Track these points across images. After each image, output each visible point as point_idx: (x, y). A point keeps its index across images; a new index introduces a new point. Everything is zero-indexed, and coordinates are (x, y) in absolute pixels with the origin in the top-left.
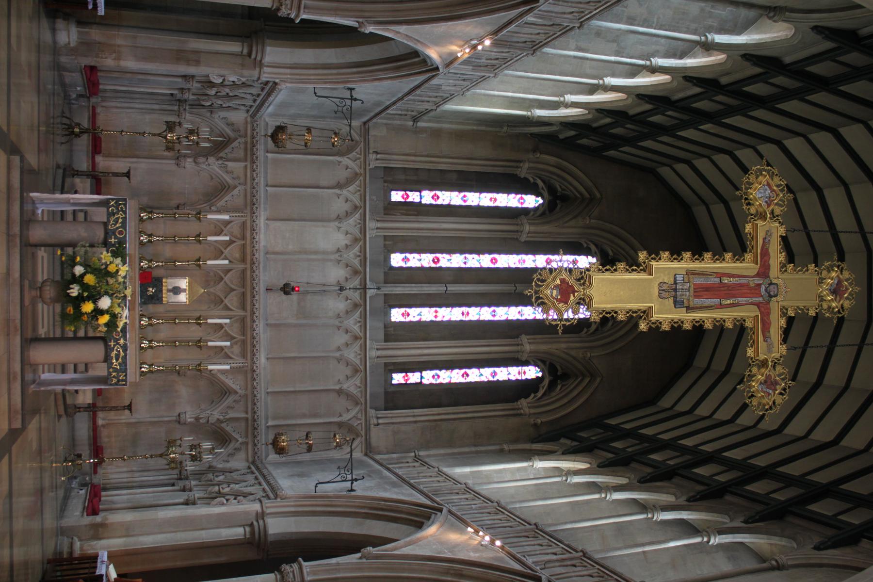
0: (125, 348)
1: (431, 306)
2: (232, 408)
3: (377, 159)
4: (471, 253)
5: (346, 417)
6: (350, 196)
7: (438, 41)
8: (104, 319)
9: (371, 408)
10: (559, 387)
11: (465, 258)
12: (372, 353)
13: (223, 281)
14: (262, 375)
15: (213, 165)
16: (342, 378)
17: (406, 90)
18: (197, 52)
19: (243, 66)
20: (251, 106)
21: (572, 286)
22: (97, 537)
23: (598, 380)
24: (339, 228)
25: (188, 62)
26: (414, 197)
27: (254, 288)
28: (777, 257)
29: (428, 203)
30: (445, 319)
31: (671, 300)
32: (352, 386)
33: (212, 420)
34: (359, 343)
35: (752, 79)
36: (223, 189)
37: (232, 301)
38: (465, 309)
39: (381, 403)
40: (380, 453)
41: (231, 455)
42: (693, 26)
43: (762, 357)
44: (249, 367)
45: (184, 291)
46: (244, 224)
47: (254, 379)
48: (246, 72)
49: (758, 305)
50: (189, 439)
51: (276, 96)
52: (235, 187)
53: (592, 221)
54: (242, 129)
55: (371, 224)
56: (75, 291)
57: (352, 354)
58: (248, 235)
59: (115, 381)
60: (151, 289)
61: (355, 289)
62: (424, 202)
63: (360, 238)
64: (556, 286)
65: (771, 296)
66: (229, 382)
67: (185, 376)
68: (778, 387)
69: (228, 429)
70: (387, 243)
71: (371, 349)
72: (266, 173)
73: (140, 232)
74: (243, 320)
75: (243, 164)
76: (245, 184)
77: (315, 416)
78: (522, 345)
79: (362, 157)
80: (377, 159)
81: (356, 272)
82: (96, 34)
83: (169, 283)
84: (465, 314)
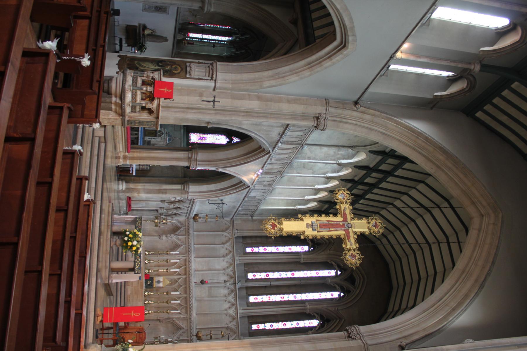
0: (140, 262)
1: (267, 295)
2: (182, 335)
3: (238, 233)
4: (282, 271)
6: (228, 247)
7: (246, 173)
8: (134, 248)
9: (241, 336)
10: (326, 325)
11: (280, 274)
12: (240, 311)
13: (177, 283)
14: (194, 320)
15: (173, 238)
16: (228, 322)
17: (242, 199)
18: (166, 190)
19: (182, 193)
20: (187, 213)
21: (276, 225)
23: (343, 320)
24: (224, 260)
25: (163, 193)
26: (256, 250)
27: (190, 285)
28: (349, 216)
29: (262, 252)
30: (274, 300)
31: (311, 229)
32: (232, 325)
34: (234, 307)
35: (365, 176)
38: (282, 296)
42: (333, 158)
43: (348, 247)
44: (189, 317)
45: (162, 282)
46: (185, 259)
47: (191, 322)
48: (183, 196)
49: (344, 230)
51: (195, 206)
52: (182, 245)
54: (184, 223)
55: (237, 258)
57: (231, 311)
58: (187, 264)
59: (137, 272)
60: (149, 281)
61: (232, 284)
62: (260, 252)
63: (232, 263)
64: (271, 225)
65: (349, 228)
66: (181, 324)
67: (162, 322)
68: (356, 257)
70: (246, 268)
72: (194, 240)
73: (145, 259)
75: (184, 237)
76: (186, 244)
78: (306, 306)
79: (232, 232)
80: (238, 233)
81: (232, 277)
82: (132, 186)
83: (156, 279)
84: (282, 297)
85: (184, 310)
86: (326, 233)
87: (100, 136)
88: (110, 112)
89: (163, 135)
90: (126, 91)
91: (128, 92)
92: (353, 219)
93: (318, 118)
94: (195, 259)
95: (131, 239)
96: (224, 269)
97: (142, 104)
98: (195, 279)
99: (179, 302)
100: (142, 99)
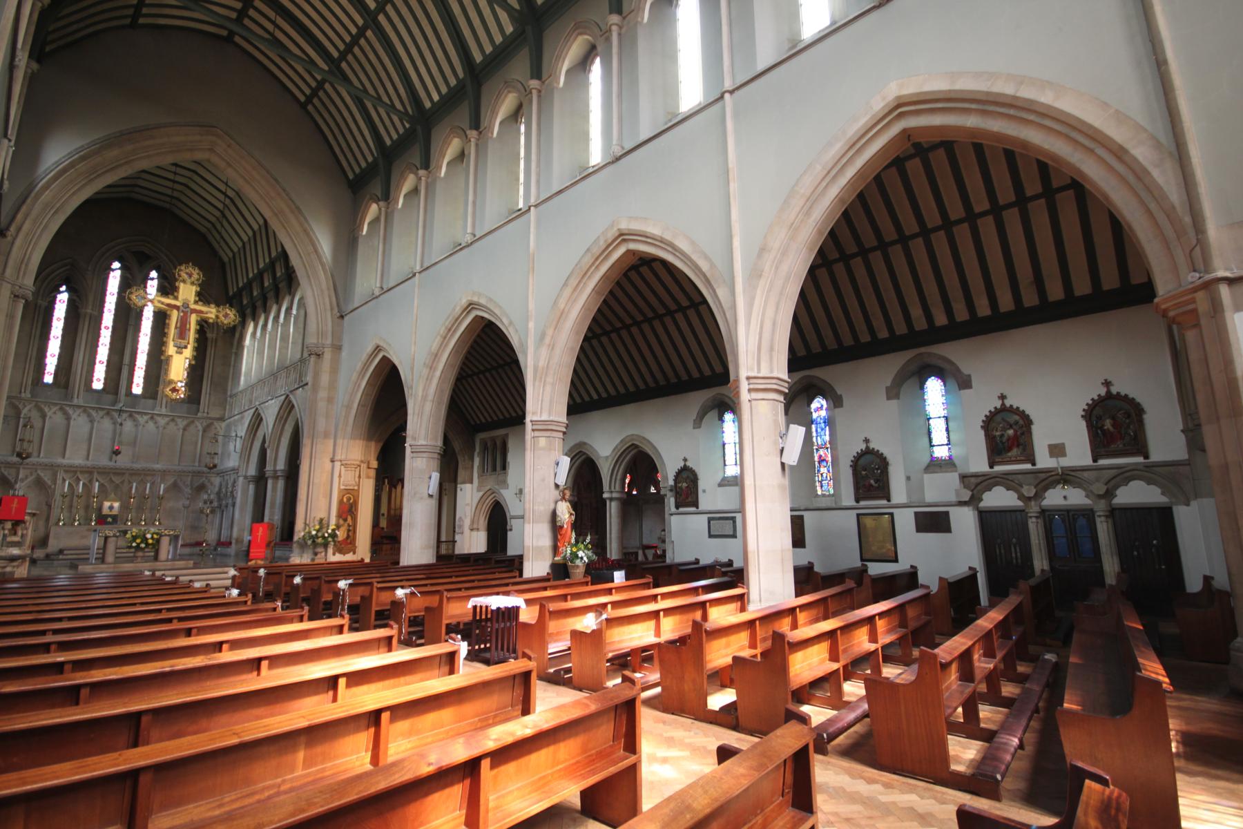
2: (184, 483)
5: (200, 428)
8: (155, 536)
9: (197, 415)
12: (164, 411)
22: (242, 541)
31: (184, 350)
32: (182, 423)
33: (190, 492)
36: (39, 483)
37: (117, 480)
39: (194, 406)
40: (224, 414)
41: (212, 484)
43: (213, 316)
49: (191, 313)
50: (201, 505)
52: (38, 475)
53: (89, 268)
55: (75, 401)
56: (143, 545)
57: (162, 421)
58: (73, 469)
63: (85, 410)
69: (196, 484)
71: (160, 411)
74: (131, 475)
77: (196, 443)
83: (105, 511)
85: (149, 478)
86: (192, 335)
92: (176, 298)
93: (15, 296)
94: (67, 456)
95: (145, 540)
96: (92, 421)
98: (104, 461)
99: (135, 484)
100: (15, 534)
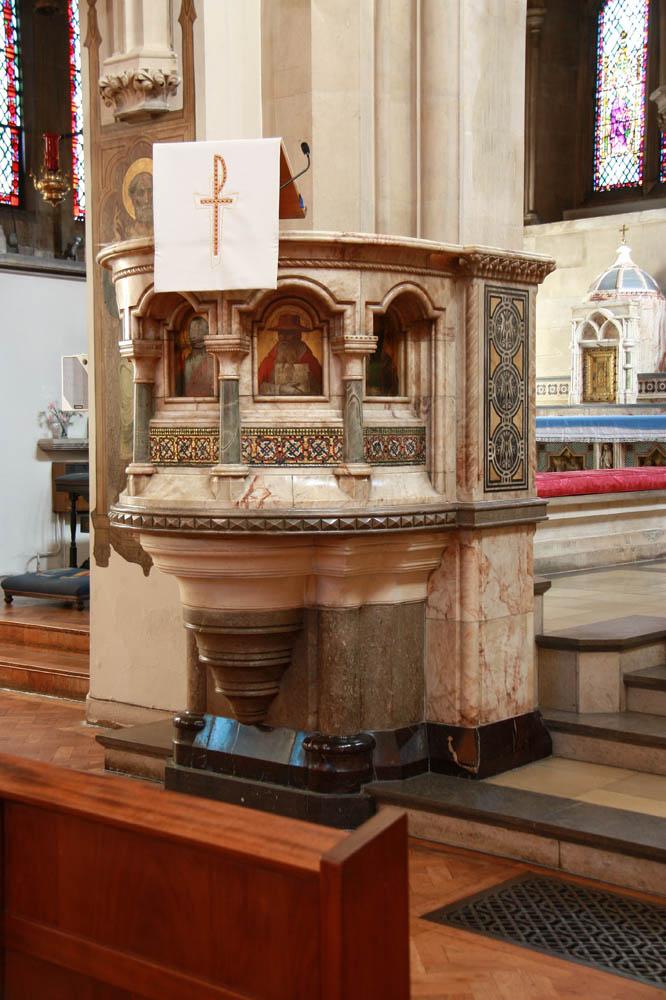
87: (616, 681)
88: (431, 614)
89: (609, 314)
90: (253, 504)
91: (258, 494)
97: (345, 384)
